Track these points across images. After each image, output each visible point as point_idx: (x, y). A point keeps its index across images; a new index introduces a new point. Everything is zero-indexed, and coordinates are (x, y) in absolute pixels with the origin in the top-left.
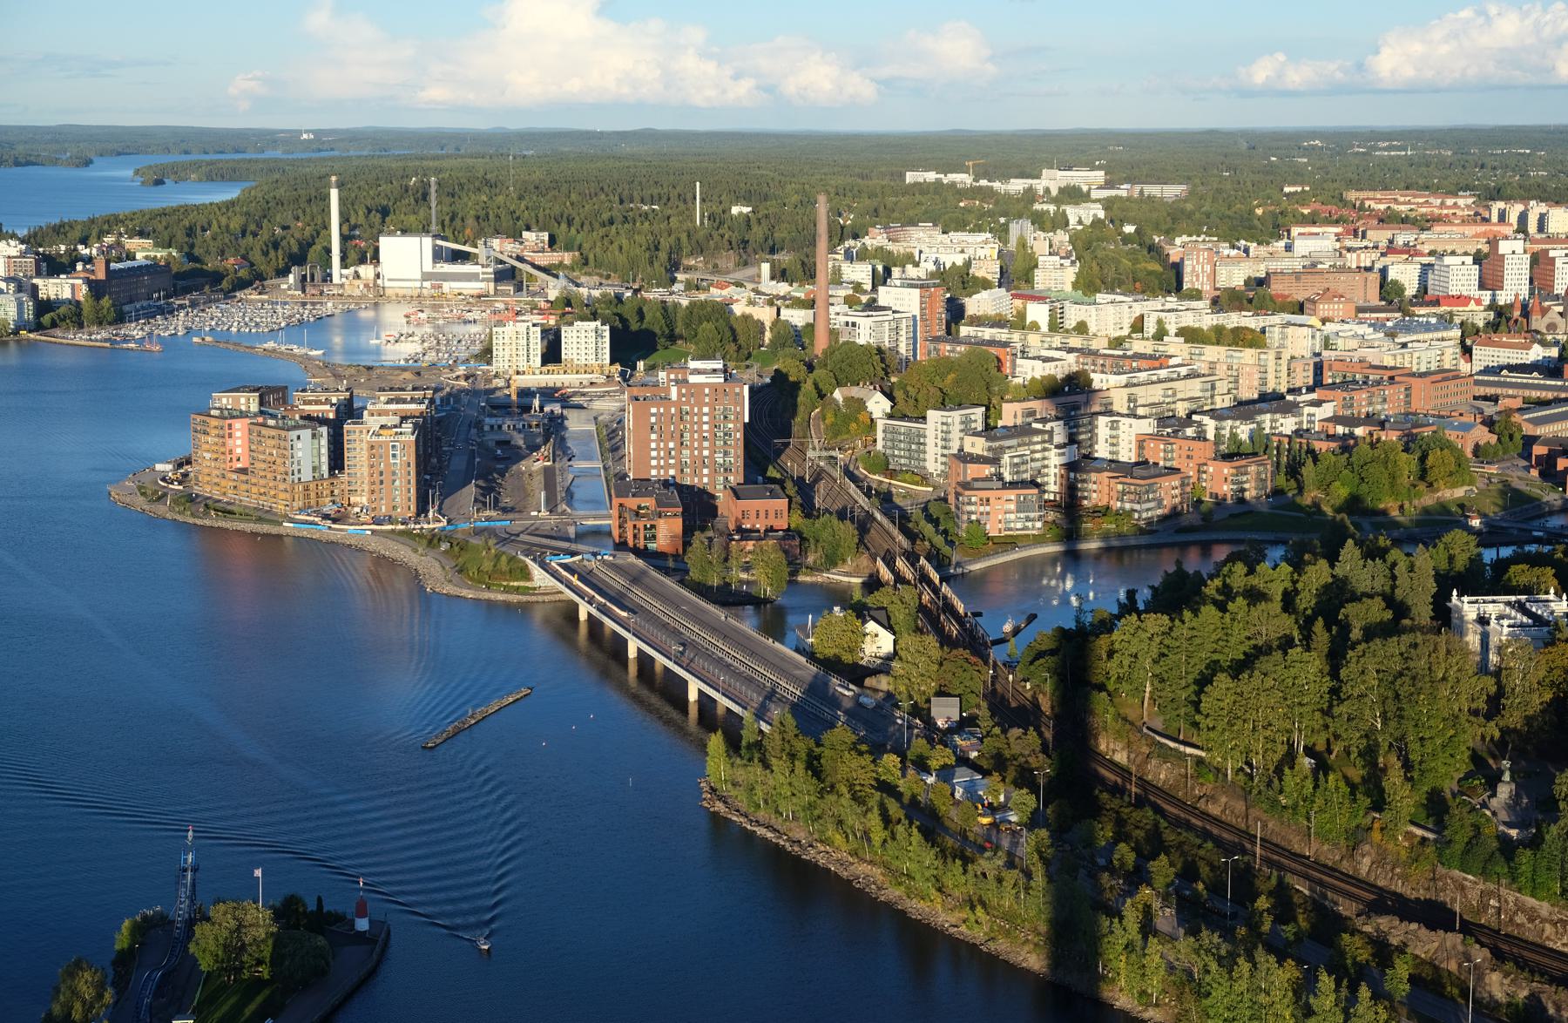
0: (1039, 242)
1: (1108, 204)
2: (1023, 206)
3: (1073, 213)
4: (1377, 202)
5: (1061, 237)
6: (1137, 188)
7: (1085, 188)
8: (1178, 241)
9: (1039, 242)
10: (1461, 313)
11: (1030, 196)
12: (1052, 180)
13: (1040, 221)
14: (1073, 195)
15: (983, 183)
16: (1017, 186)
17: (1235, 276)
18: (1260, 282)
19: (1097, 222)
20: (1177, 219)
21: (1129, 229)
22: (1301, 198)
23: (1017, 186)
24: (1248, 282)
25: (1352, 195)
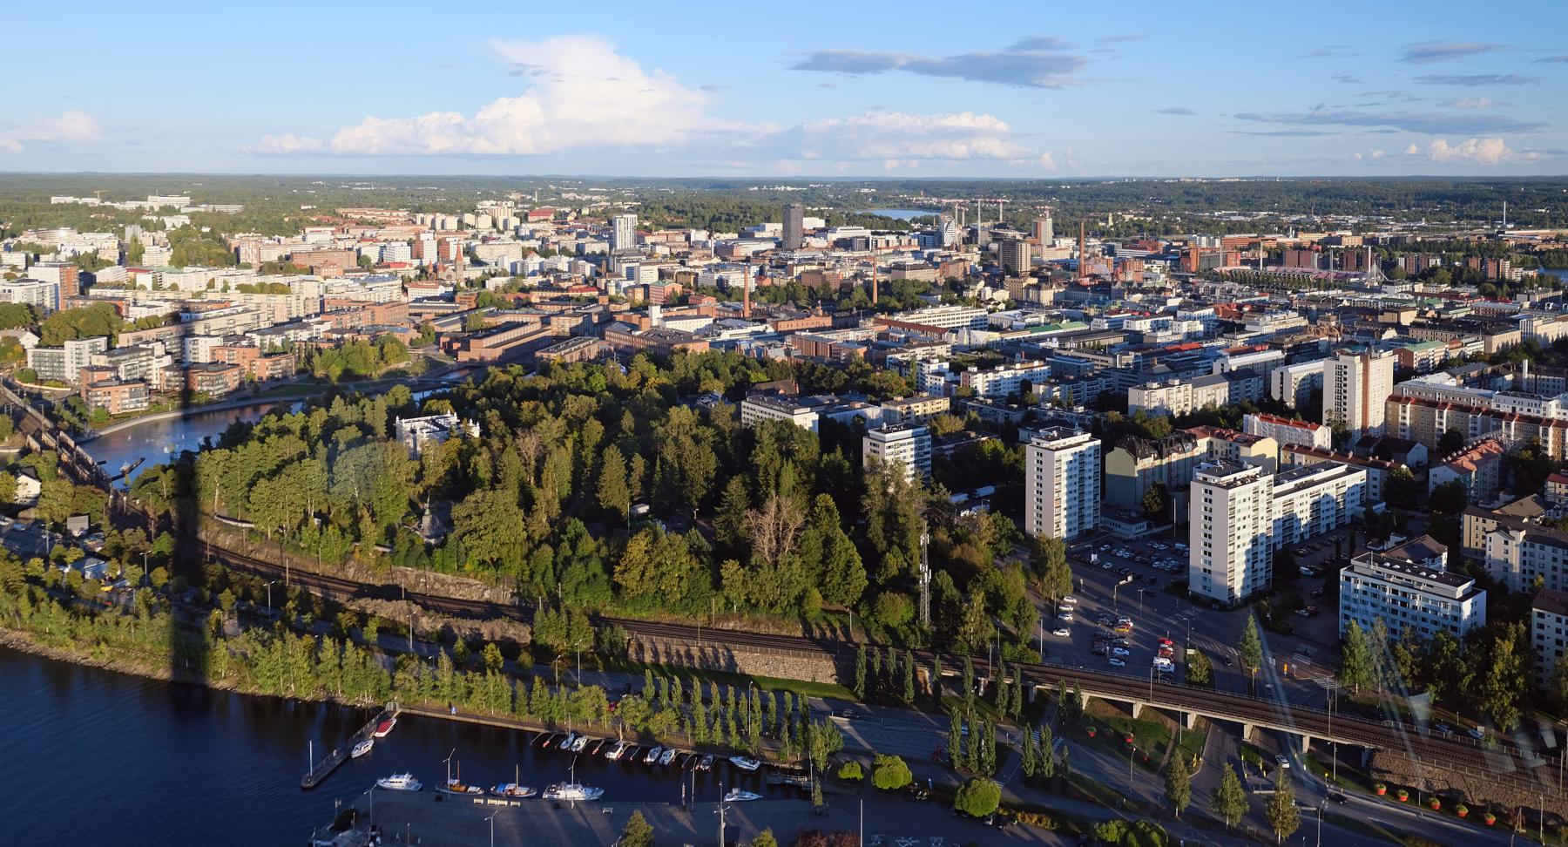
0: (146, 238)
1: (192, 216)
2: (136, 217)
3: (169, 221)
4: (355, 214)
5: (161, 235)
6: (211, 207)
7: (177, 207)
8: (237, 236)
9: (146, 238)
10: (402, 271)
11: (140, 211)
12: (155, 202)
13: (146, 226)
14: (170, 211)
15: (108, 203)
16: (131, 205)
17: (272, 255)
18: (288, 258)
19: (185, 227)
20: (235, 224)
21: (206, 230)
22: (312, 212)
23: (131, 205)
24: (280, 258)
25: (341, 211)
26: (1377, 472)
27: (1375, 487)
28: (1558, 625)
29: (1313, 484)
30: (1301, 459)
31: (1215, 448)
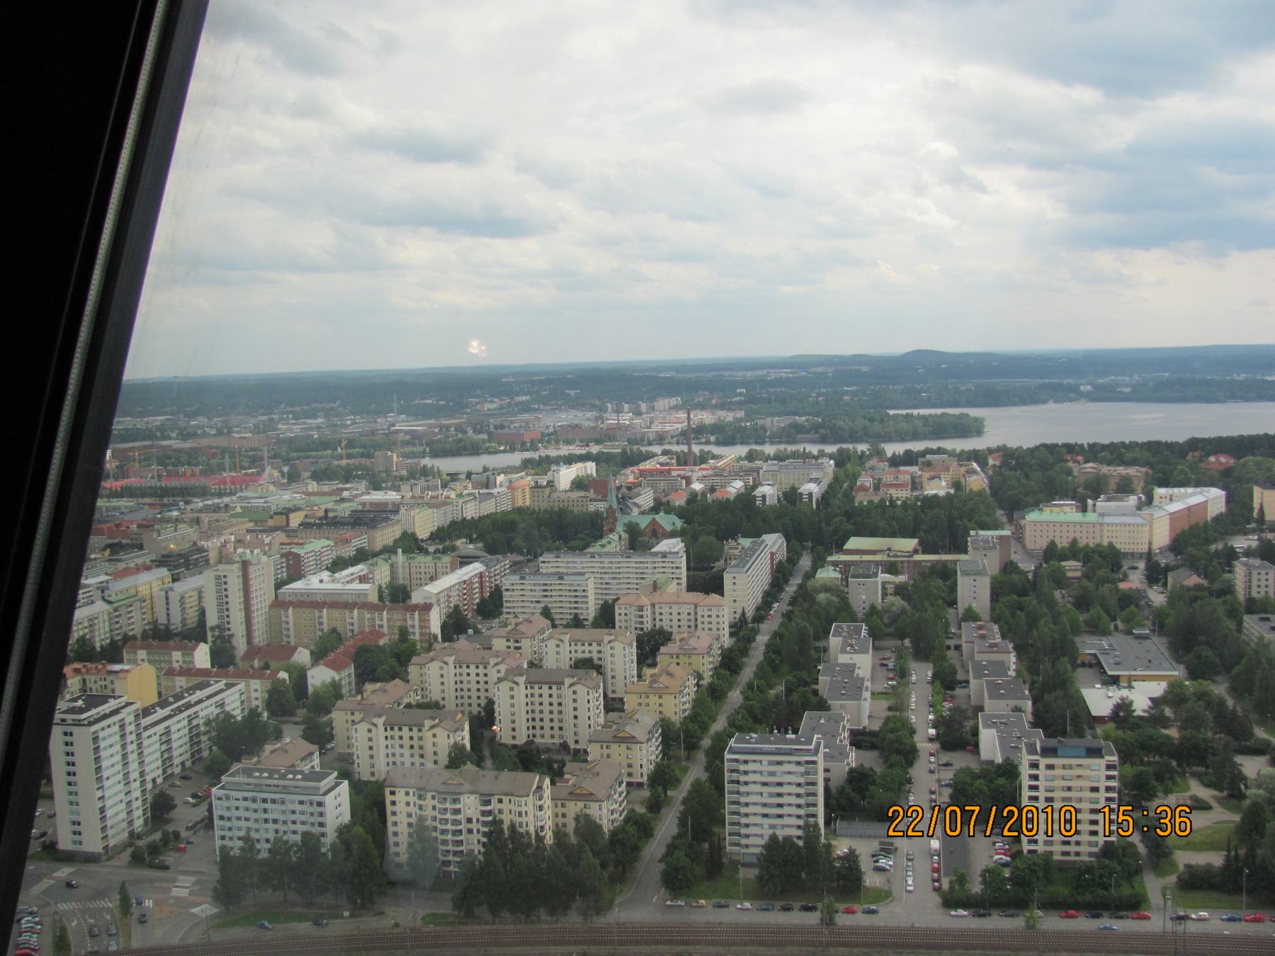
26: (256, 684)
27: (257, 699)
28: (407, 799)
29: (188, 706)
30: (181, 682)
31: (89, 685)
